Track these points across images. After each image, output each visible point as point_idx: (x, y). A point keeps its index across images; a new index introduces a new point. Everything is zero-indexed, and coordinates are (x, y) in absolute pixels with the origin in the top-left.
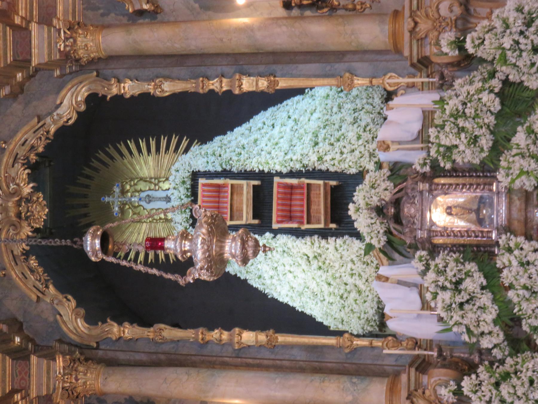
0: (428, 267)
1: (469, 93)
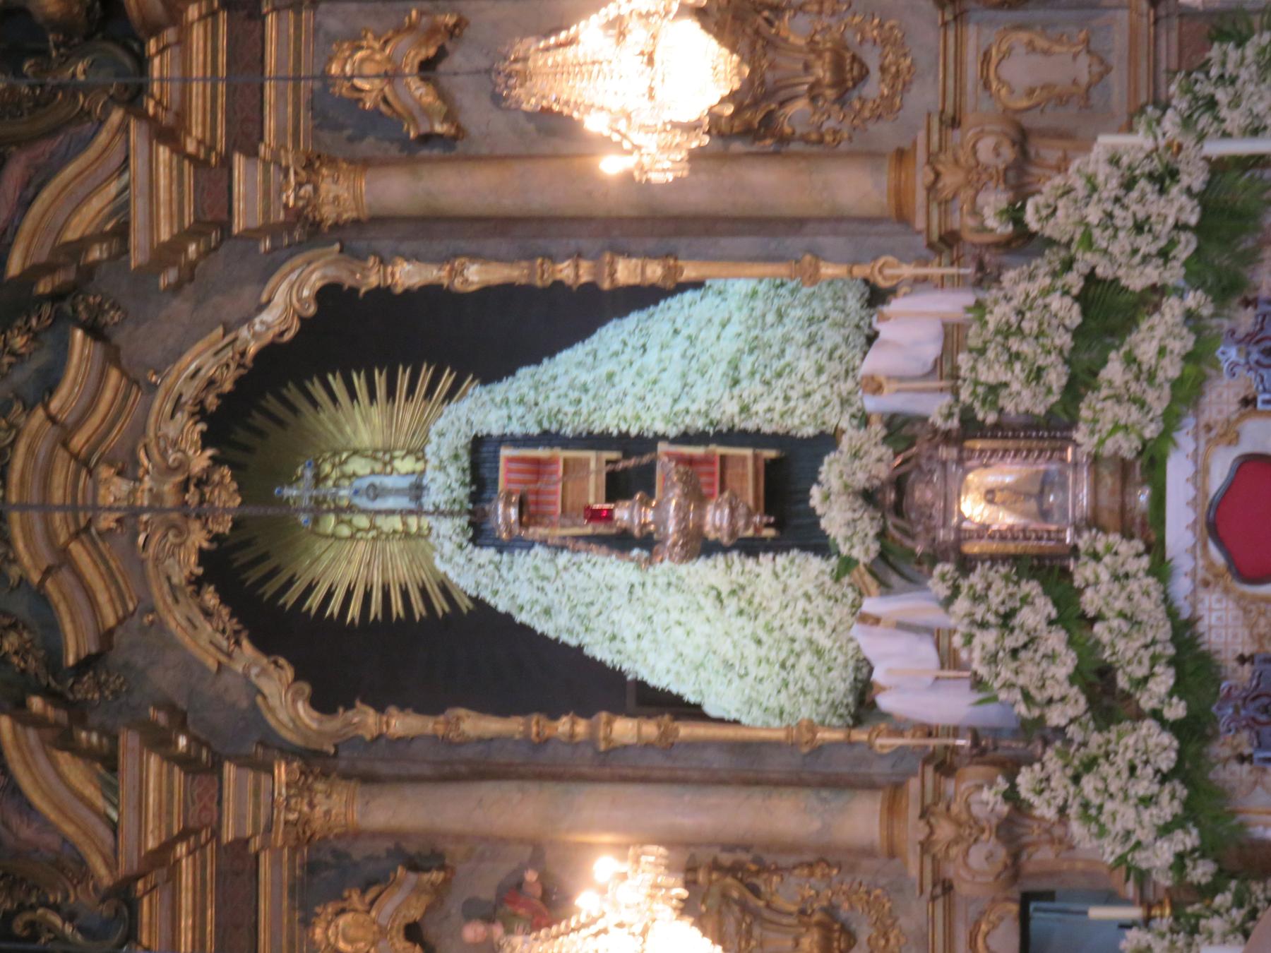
0: (956, 591)
1: (1028, 295)
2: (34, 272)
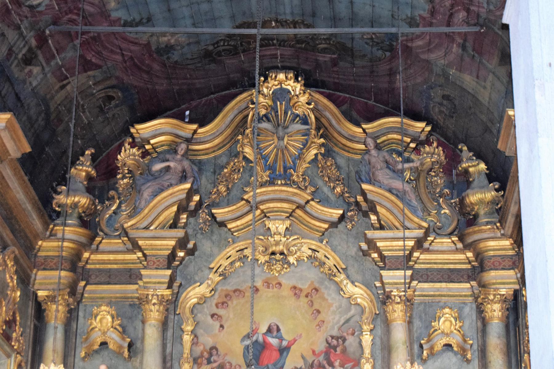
2: (363, 193)
